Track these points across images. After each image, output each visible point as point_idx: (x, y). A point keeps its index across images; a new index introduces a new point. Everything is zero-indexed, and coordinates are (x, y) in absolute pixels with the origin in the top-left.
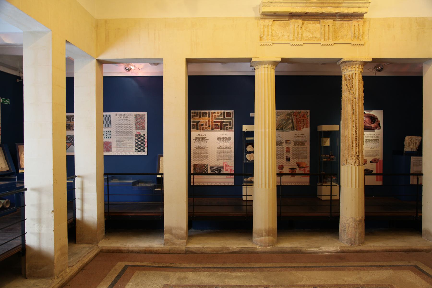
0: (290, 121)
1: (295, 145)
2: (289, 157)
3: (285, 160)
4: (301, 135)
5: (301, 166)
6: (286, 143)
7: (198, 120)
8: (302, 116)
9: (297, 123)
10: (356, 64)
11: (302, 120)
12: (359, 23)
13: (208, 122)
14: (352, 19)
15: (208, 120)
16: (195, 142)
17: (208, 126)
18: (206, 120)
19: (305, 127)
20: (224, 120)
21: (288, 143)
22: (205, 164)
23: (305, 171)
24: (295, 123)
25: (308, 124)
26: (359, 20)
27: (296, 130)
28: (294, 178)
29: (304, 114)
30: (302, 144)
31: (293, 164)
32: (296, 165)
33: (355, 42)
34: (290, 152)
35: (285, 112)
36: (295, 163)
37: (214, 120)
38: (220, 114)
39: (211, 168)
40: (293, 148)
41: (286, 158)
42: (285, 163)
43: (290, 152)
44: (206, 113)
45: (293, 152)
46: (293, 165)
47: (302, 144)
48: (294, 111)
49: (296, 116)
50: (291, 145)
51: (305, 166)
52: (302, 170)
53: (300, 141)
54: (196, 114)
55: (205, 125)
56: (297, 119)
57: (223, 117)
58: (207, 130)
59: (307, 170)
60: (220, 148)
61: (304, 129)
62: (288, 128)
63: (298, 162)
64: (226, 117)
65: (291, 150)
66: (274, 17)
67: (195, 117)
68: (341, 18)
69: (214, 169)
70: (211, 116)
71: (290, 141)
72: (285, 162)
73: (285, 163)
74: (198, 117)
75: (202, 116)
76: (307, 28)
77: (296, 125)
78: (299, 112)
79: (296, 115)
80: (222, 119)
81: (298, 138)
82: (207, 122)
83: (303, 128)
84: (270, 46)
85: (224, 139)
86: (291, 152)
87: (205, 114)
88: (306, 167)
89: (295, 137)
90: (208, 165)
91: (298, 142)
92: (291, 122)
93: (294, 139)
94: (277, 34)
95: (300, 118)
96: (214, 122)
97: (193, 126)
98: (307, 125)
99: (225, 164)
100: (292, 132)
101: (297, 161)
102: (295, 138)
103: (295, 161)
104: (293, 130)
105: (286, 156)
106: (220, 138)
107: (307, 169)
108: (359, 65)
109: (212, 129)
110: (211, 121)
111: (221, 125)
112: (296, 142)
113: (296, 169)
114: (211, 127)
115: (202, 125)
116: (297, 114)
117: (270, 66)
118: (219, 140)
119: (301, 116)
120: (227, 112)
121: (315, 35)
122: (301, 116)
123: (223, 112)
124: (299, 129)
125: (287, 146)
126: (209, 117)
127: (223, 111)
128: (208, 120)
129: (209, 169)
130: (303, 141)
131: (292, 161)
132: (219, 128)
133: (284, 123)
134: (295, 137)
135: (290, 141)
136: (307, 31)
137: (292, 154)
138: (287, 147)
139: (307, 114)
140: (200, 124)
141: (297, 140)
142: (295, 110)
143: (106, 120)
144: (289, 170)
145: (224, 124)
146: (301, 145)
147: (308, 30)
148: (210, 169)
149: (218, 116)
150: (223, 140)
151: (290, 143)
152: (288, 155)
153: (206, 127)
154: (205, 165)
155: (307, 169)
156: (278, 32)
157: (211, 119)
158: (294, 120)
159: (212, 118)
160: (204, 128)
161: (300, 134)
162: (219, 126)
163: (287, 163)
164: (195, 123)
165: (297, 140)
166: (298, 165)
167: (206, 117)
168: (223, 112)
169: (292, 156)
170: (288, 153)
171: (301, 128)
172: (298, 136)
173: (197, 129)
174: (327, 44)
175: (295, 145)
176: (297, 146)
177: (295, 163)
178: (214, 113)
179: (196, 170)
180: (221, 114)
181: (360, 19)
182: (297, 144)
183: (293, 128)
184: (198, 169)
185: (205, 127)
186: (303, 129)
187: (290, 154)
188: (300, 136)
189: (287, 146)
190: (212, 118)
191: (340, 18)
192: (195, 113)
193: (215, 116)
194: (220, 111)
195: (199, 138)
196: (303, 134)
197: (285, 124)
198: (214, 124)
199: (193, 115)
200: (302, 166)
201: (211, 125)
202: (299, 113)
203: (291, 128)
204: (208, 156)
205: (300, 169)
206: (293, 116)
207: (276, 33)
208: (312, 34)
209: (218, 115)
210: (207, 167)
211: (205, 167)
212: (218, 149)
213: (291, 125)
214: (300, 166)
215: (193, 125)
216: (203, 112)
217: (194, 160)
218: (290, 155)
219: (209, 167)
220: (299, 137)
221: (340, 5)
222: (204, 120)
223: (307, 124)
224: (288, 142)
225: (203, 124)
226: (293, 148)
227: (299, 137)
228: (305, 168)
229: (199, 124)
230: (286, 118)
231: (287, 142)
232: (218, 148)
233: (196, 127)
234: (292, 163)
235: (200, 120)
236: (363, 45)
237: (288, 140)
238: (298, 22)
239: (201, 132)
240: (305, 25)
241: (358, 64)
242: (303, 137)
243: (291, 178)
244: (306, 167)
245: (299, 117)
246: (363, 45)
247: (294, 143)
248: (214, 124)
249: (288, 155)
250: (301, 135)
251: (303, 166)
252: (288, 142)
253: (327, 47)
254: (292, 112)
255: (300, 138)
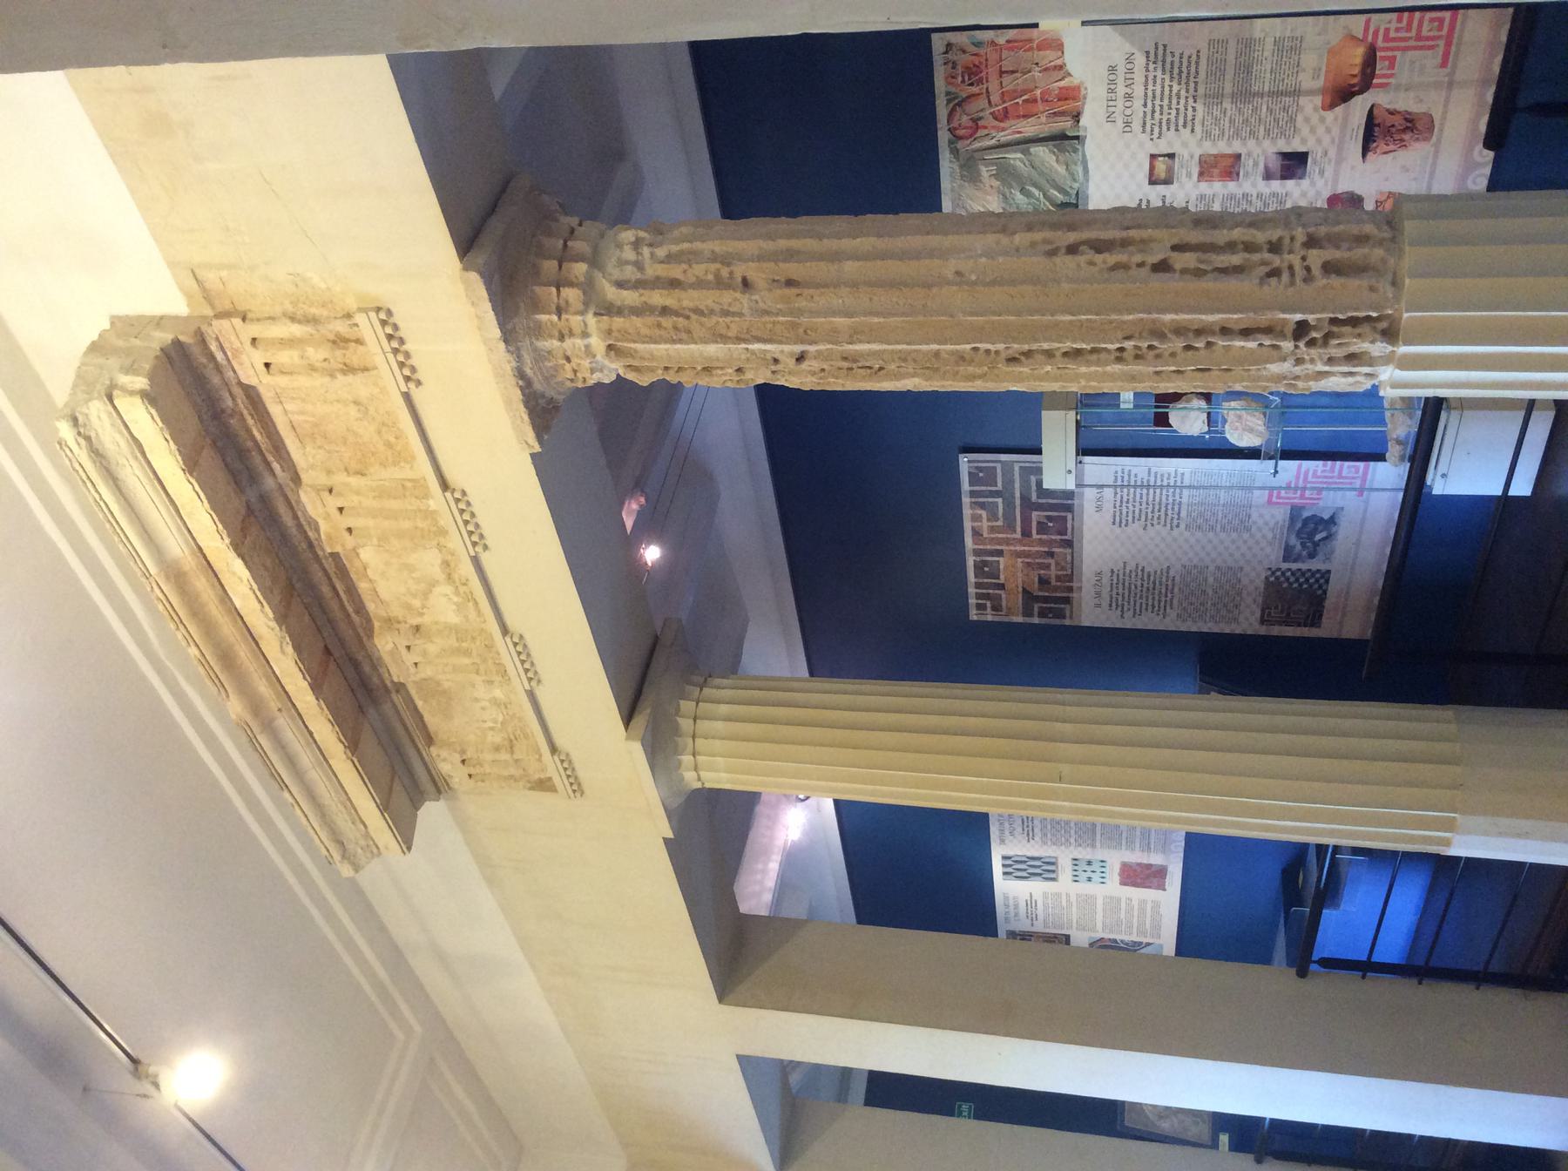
0: (1015, 157)
1: (1185, 126)
2: (1274, 157)
3: (1290, 184)
4: (1112, 82)
5: (1355, 76)
6: (1168, 181)
7: (1020, 596)
8: (980, 81)
9: (1026, 116)
10: (540, 357)
11: (1007, 79)
12: (237, 344)
13: (1029, 560)
14: (234, 399)
15: (1020, 560)
16: (1135, 613)
17: (1052, 562)
18: (1020, 565)
19: (1059, 62)
20: (1018, 495)
21: (1170, 170)
22: (1267, 578)
23: (1403, 44)
24: (1029, 128)
25: (1031, 41)
26: (219, 356)
27: (1077, 117)
28: (1442, 125)
29: (960, 70)
30: (1181, 72)
31: (1328, 130)
32: (1339, 110)
33: (375, 348)
34: (1238, 157)
35: (952, 190)
36: (1329, 116)
37: (1018, 535)
38: (984, 514)
39: (1288, 555)
40: (1207, 135)
41: (1284, 178)
42: (1313, 184)
43: (1238, 157)
44: (979, 568)
45: (1237, 134)
46: (1336, 131)
47: (1181, 72)
48: (943, 136)
49: (975, 121)
50: (1189, 146)
51: (1358, 54)
52: (1392, 66)
53: (1158, 89)
54: (989, 604)
55: (1042, 572)
56: (1004, 116)
57: (1000, 500)
58: (1069, 566)
59: (1397, 30)
60: (1176, 517)
61: (1069, 67)
62: (1061, 170)
63: (1318, 100)
64: (1000, 486)
65: (1222, 147)
66: (411, 752)
67: (1001, 606)
68: (261, 468)
69: (1299, 547)
70: (999, 547)
71: (1153, 157)
72: (1305, 183)
73: (1320, 183)
74: (1004, 596)
75: (999, 578)
76: (409, 607)
77: (1043, 119)
78: (949, 101)
79: (970, 124)
80: (1009, 505)
81: (1138, 103)
82: (1028, 563)
83: (1061, 74)
84: (575, 757)
85: (1125, 499)
86: (1237, 147)
87: (986, 569)
88: (1370, 38)
89: (1128, 124)
90: (1270, 569)
91: (1166, 102)
92: (1019, 155)
93: (1144, 132)
94: (499, 725)
95: (995, 98)
96: (1026, 533)
97: (1051, 615)
98: (1040, 48)
99: (1274, 500)
100: (1090, 147)
101: (1310, 105)
102: (1137, 126)
103: (1307, 120)
104: (1077, 138)
105: (1268, 176)
106: (1118, 514)
107: (1387, 30)
108: (538, 331)
109: (1069, 544)
110: (1019, 548)
111: (1040, 507)
112: (1165, 118)
113: (1373, 106)
114: (1054, 550)
115: (1043, 582)
116: (965, 118)
117: (687, 759)
118: (1130, 518)
119: (975, 90)
120: (971, 484)
121: (437, 572)
122: (975, 90)
123: (973, 500)
124: (1069, 102)
125: (1189, 175)
126: (1000, 553)
127: (966, 500)
128: (1020, 557)
129: (1294, 566)
130: (1160, 64)
131: (1304, 141)
132: (1065, 518)
133: (1028, 194)
134: (1128, 124)
135: (1153, 157)
136: (424, 607)
137: (1251, 143)
138: (1201, 174)
139: (964, 52)
140: (1040, 590)
141: (1153, 112)
142: (939, 133)
143: (1027, 867)
144: (1370, 155)
145: (1038, 497)
146: (1192, 79)
147: (417, 603)
148: (1295, 561)
149: (993, 516)
150: (1127, 502)
151: (1171, 156)
152: (1256, 164)
153: (1053, 567)
154: (1272, 579)
155: (1387, 30)
156: (485, 722)
157: (1012, 548)
158: (1005, 137)
159: (1007, 542)
160: (1058, 578)
161: (1112, 91)
162: (1049, 518)
163: (1322, 173)
164: (1036, 610)
165: (1153, 112)
166: (1341, 94)
167: (1002, 567)
168: (973, 500)
169: (1267, 143)
170: (1247, 164)
171: (1060, 88)
172: (1120, 103)
173: (1067, 600)
174: (466, 523)
175: (1185, 126)
176: (1194, 109)
177: (1322, 120)
178: (976, 533)
179: (1292, 615)
180: (982, 506)
181: (213, 347)
182: (1181, 107)
183: (1065, 141)
184: (1289, 608)
185: (1053, 572)
186: (1070, 75)
187: (1249, 155)
188: (1121, 90)
189: (1189, 175)
190: (1007, 542)
191: (266, 474)
192: (980, 607)
193: (992, 529)
194: (967, 512)
195: (1114, 596)
196: (1112, 69)
197: (1036, 192)
198: (1035, 536)
199: (994, 613)
200: (1356, 71)
201: (1046, 549)
202: (959, 104)
203: (1062, 150)
204: (1218, 568)
205: (1375, 81)
206: (977, 145)
207: (492, 729)
208: (434, 586)
209: (989, 520)
210: (1283, 574)
211: (1282, 579)
212: (1183, 526)
213: (1042, 152)
214: (1355, 81)
215: (1042, 614)
216: (976, 577)
217: (1236, 620)
218: (1261, 151)
219: (1285, 566)
220: (1128, 97)
221: (186, 568)
222: (1020, 574)
223: (1031, 49)
224: (1161, 166)
225: (1036, 579)
226: (1207, 135)
227: (1128, 97)
228: (1380, 43)
229: (1041, 594)
230: (996, 183)
231: (1163, 176)
232: (1178, 526)
233: (1052, 605)
234: (1319, 141)
235: (1020, 589)
236: (383, 316)
237: (1152, 168)
238: (394, 652)
239: (1080, 588)
240: (396, 611)
241: (535, 350)
242: (1130, 71)
243: (1437, 146)
244: (1370, 38)
245: (983, 103)
246: (383, 316)
247: (1173, 128)
248: (1039, 537)
249: (1261, 166)
250: (1112, 82)
251: (1358, 60)
252: (1161, 166)
253: (480, 519)
254: (955, 152)
255: (1139, 90)
